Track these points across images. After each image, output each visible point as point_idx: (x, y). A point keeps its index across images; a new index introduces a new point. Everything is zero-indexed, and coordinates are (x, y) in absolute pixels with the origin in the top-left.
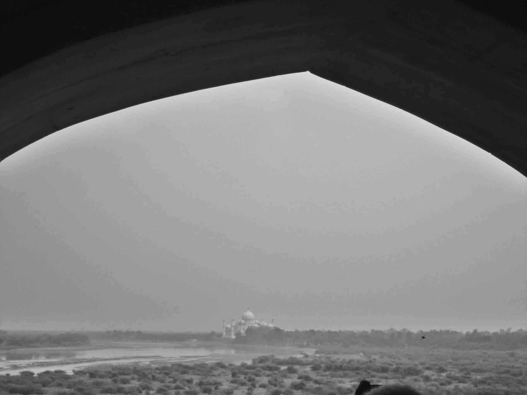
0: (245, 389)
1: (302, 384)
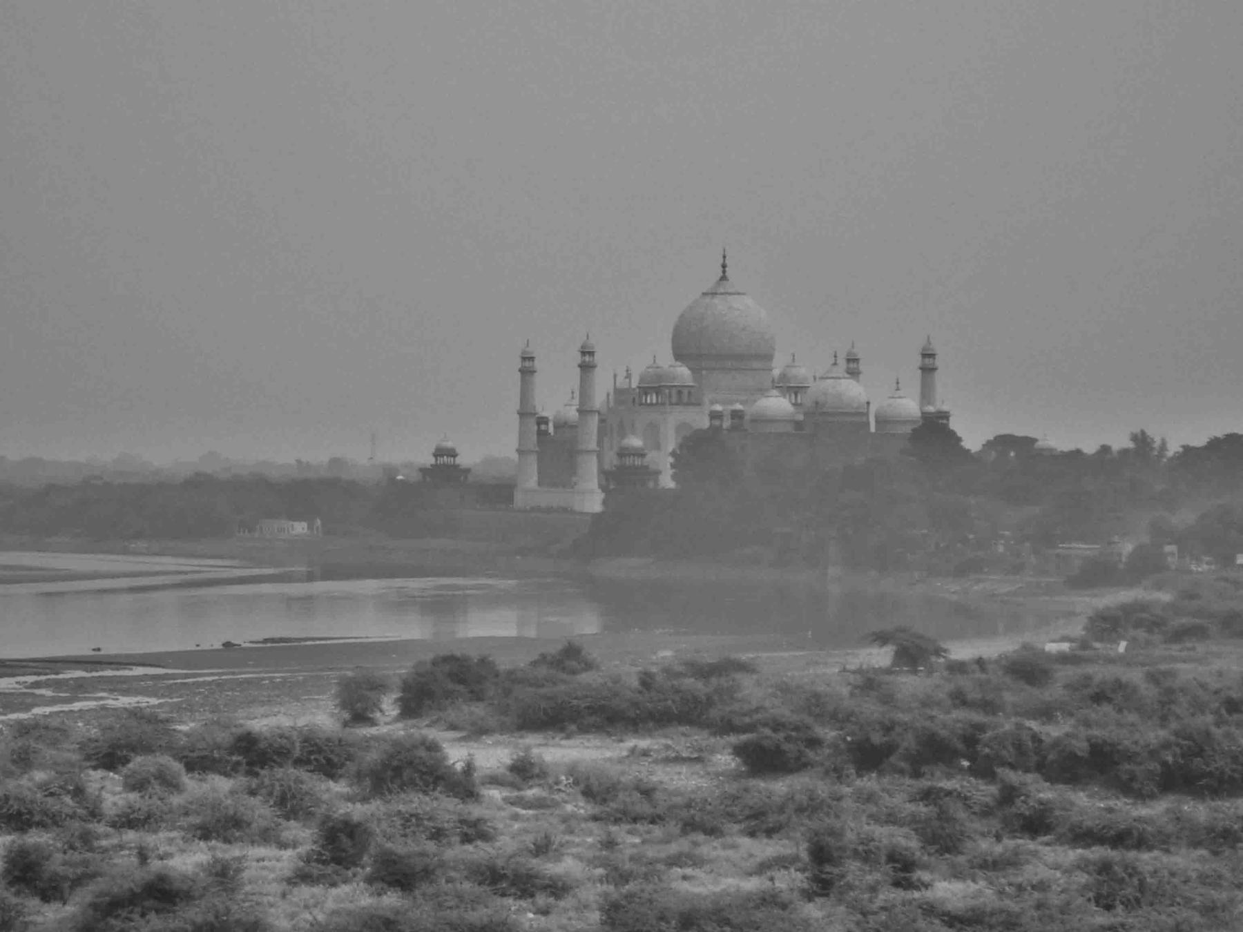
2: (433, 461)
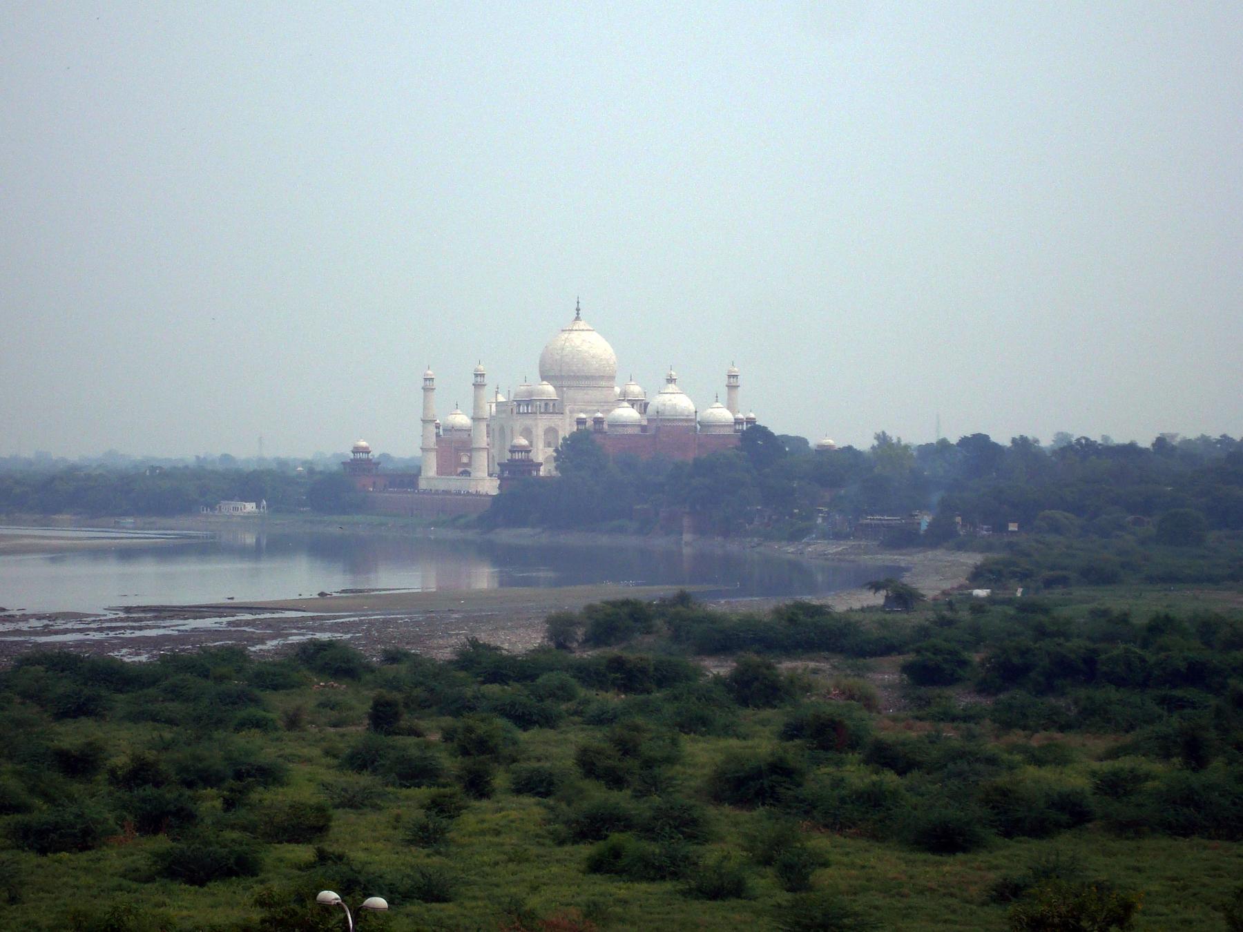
0: (411, 803)
1: (779, 769)
2: (352, 456)
